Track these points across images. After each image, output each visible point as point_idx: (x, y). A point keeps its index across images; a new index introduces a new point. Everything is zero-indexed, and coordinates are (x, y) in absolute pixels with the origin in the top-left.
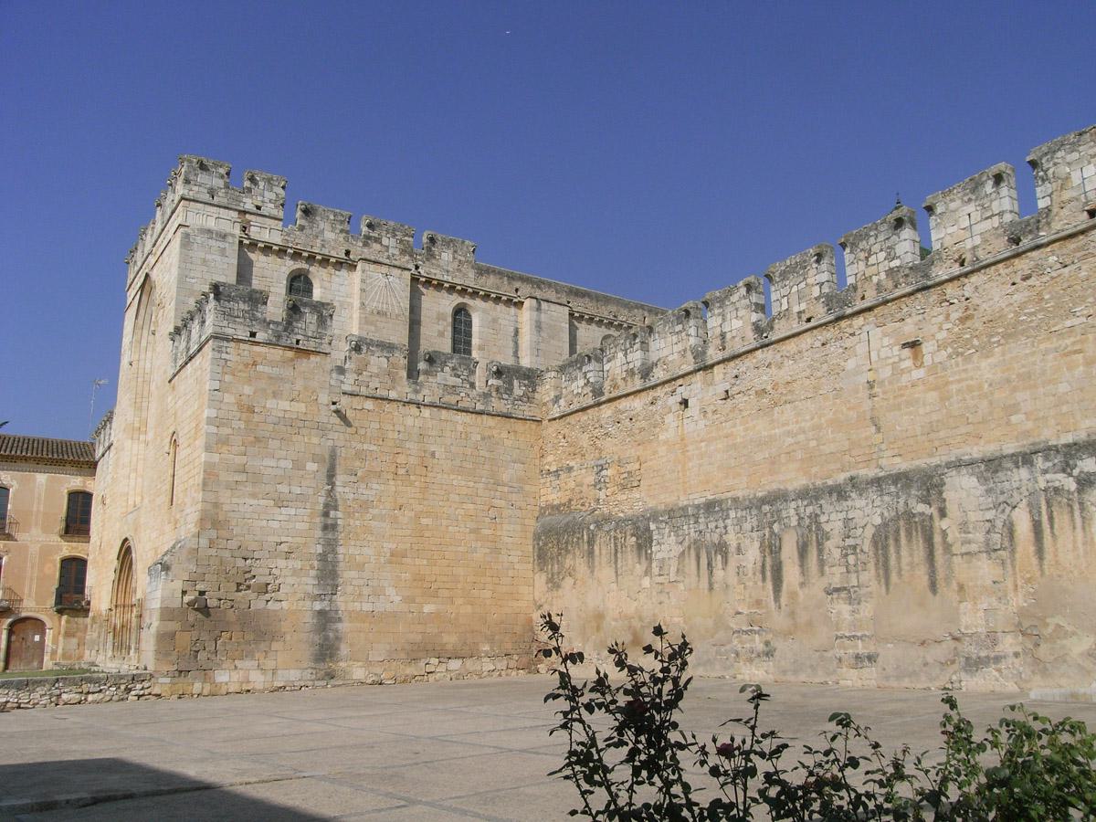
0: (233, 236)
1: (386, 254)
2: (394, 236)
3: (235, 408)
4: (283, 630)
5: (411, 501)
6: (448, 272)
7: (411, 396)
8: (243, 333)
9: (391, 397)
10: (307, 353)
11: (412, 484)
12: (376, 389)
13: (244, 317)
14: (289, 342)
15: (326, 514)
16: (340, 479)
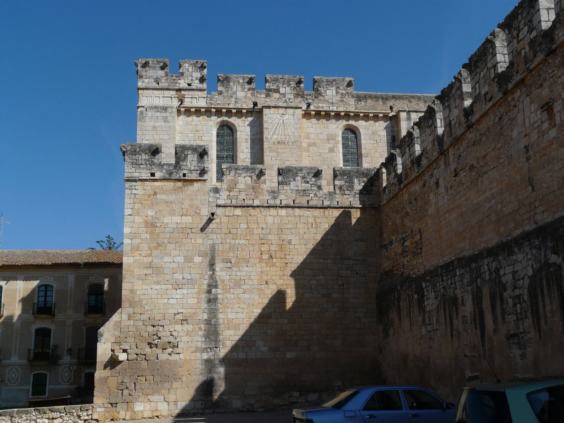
0: (172, 107)
1: (284, 99)
2: (289, 85)
3: (143, 226)
4: (180, 374)
5: (274, 278)
6: (333, 104)
7: (271, 202)
8: (145, 175)
9: (255, 204)
10: (192, 181)
11: (274, 265)
12: (244, 200)
13: (146, 164)
14: (178, 176)
15: (209, 292)
16: (218, 266)
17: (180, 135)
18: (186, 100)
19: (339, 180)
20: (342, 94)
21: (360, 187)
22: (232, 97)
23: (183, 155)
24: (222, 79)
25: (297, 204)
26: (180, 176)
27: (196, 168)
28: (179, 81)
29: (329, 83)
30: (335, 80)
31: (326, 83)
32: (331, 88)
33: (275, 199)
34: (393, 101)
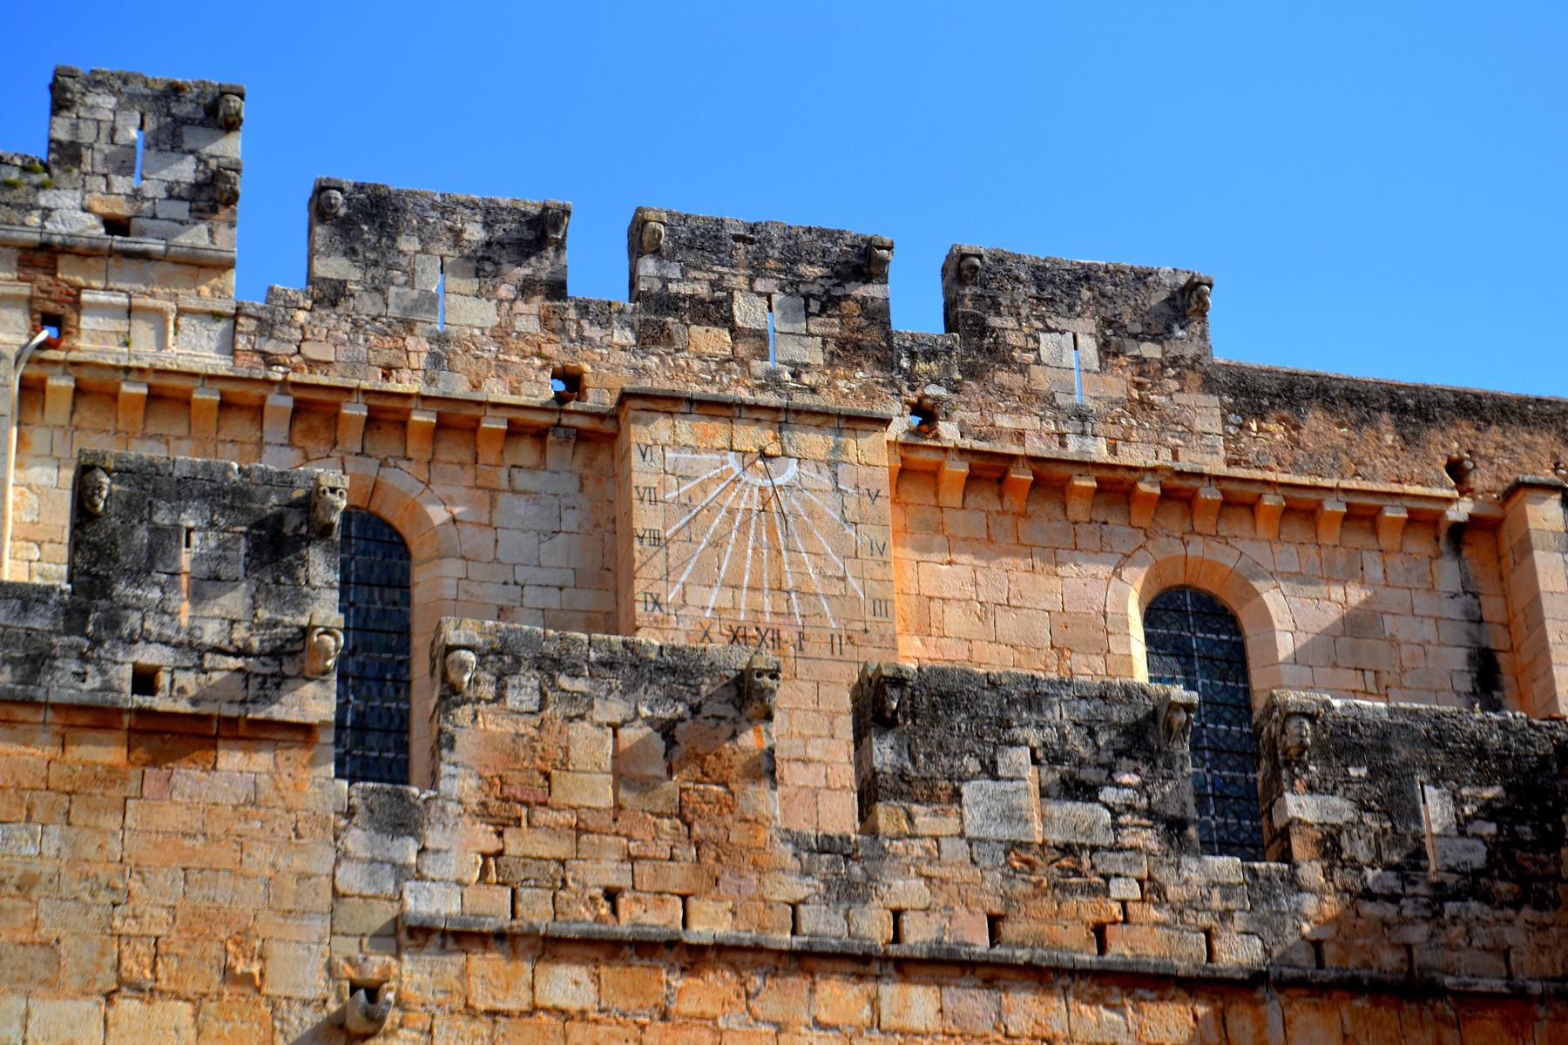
6: (1082, 415)
12: (612, 895)
14: (93, 682)
17: (36, 554)
18: (87, 322)
19: (1311, 788)
20: (1140, 361)
21: (1468, 850)
22: (409, 325)
23: (142, 535)
24: (342, 211)
25: (1023, 945)
26: (107, 687)
27: (240, 633)
28: (44, 199)
29: (1050, 288)
30: (1087, 278)
31: (1033, 291)
32: (1064, 323)
33: (851, 898)
34: (1466, 429)
